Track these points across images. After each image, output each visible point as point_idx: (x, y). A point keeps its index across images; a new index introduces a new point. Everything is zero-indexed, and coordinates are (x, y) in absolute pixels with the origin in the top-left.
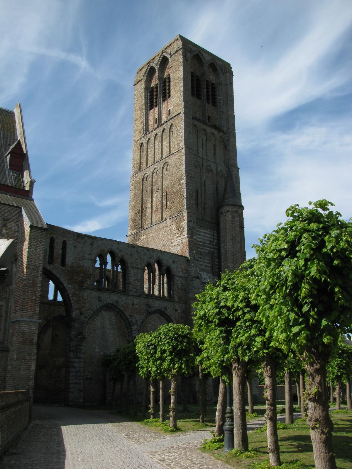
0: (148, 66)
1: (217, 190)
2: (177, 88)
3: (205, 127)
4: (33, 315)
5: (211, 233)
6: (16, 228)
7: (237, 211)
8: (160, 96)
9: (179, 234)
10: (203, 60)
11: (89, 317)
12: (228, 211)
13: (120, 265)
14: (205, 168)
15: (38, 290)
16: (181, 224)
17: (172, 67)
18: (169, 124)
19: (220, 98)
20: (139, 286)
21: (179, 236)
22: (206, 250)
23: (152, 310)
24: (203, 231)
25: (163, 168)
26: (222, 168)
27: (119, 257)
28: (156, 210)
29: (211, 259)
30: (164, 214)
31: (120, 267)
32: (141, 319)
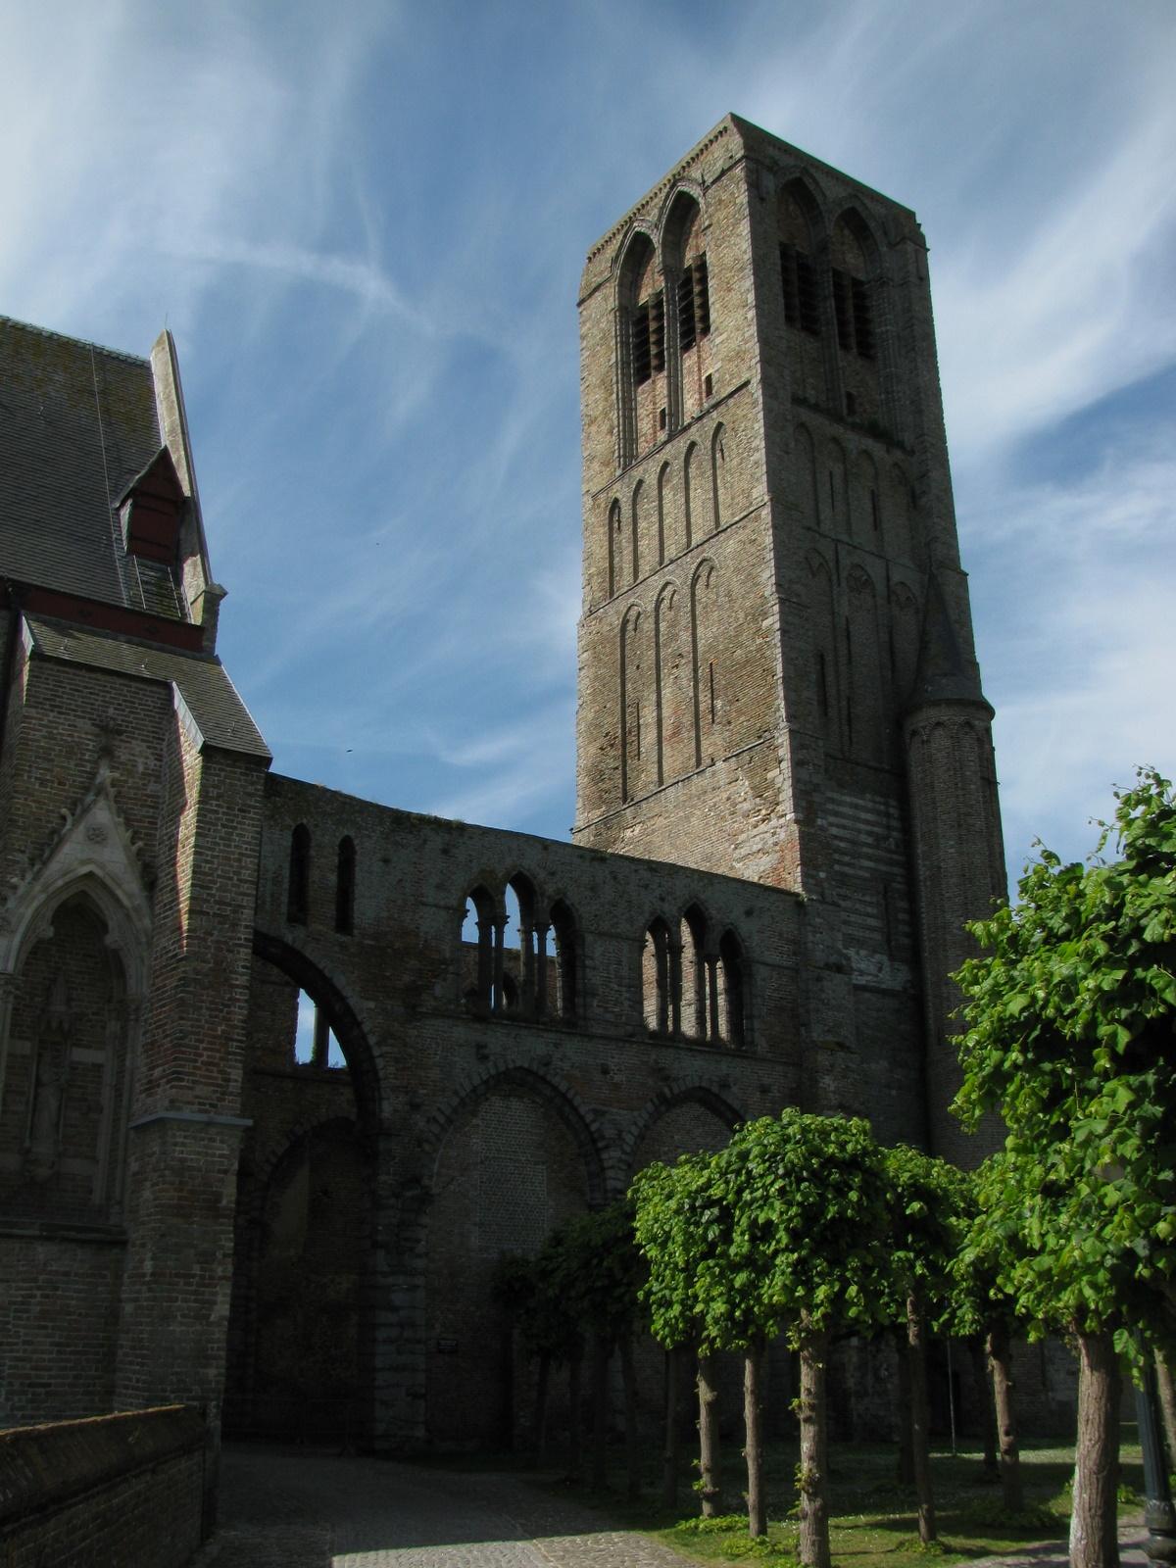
0: (627, 232)
1: (892, 652)
2: (734, 297)
3: (838, 430)
4: (219, 1100)
5: (877, 806)
6: (152, 763)
7: (968, 724)
8: (672, 331)
9: (764, 812)
10: (819, 199)
11: (442, 1120)
12: (939, 724)
13: (552, 927)
14: (844, 574)
15: (238, 1000)
16: (770, 775)
17: (710, 226)
18: (710, 424)
19: (887, 331)
20: (626, 1003)
21: (764, 821)
22: (861, 868)
23: (676, 1091)
24: (848, 799)
25: (695, 579)
26: (904, 573)
27: (549, 897)
28: (676, 733)
29: (882, 902)
30: (704, 744)
31: (551, 934)
32: (635, 1124)
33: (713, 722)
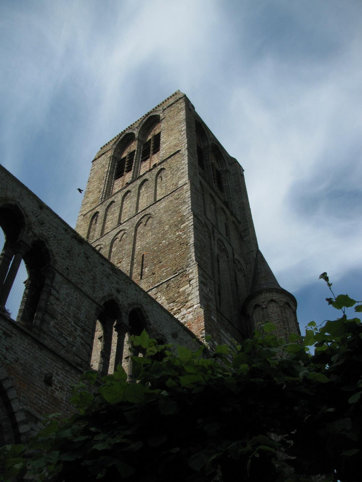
12: (272, 301)
20: (78, 339)
27: (35, 235)
33: (141, 278)
